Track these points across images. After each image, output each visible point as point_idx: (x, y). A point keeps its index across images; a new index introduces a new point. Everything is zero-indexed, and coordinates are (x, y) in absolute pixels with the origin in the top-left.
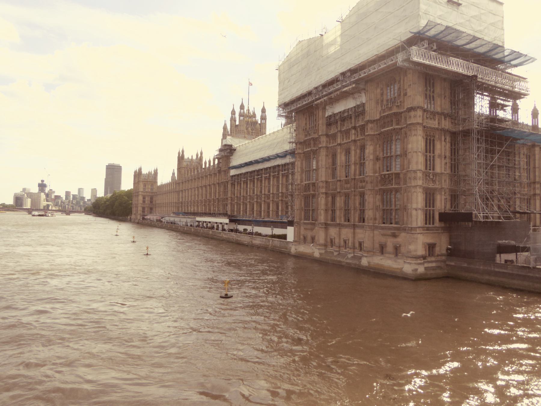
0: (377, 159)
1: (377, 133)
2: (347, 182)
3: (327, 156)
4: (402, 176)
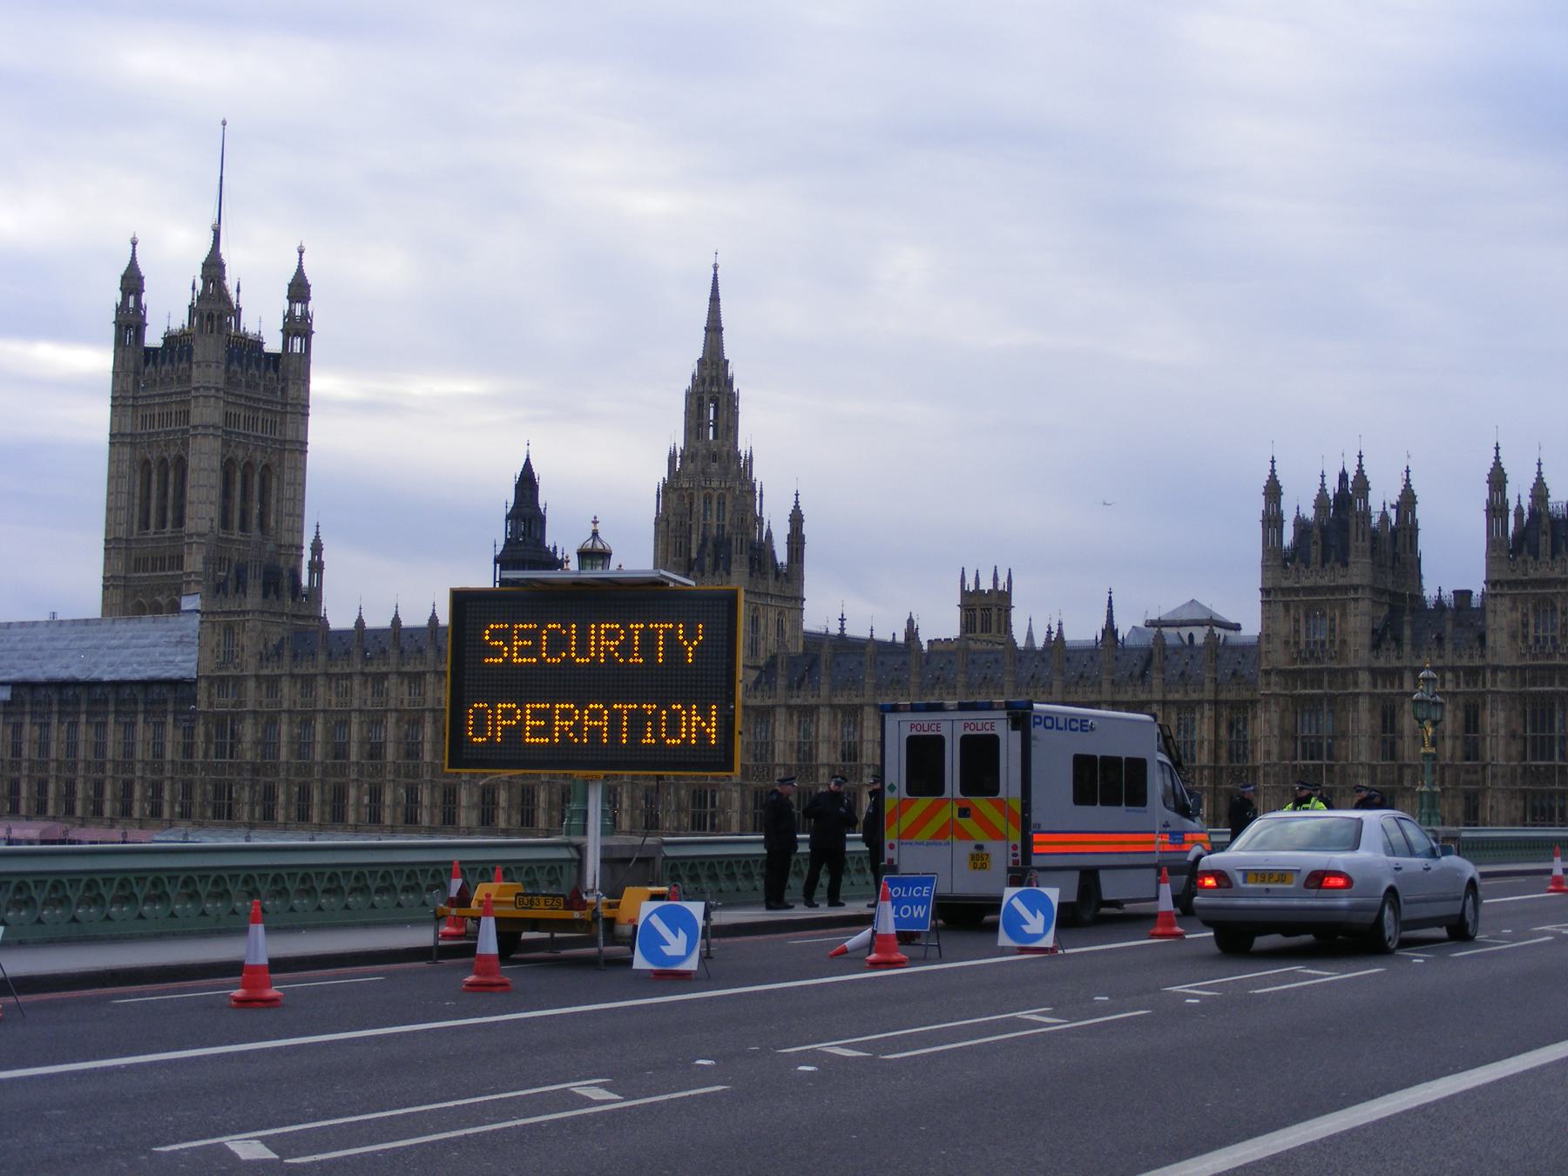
0: (1513, 735)
1: (1517, 690)
3: (1371, 710)
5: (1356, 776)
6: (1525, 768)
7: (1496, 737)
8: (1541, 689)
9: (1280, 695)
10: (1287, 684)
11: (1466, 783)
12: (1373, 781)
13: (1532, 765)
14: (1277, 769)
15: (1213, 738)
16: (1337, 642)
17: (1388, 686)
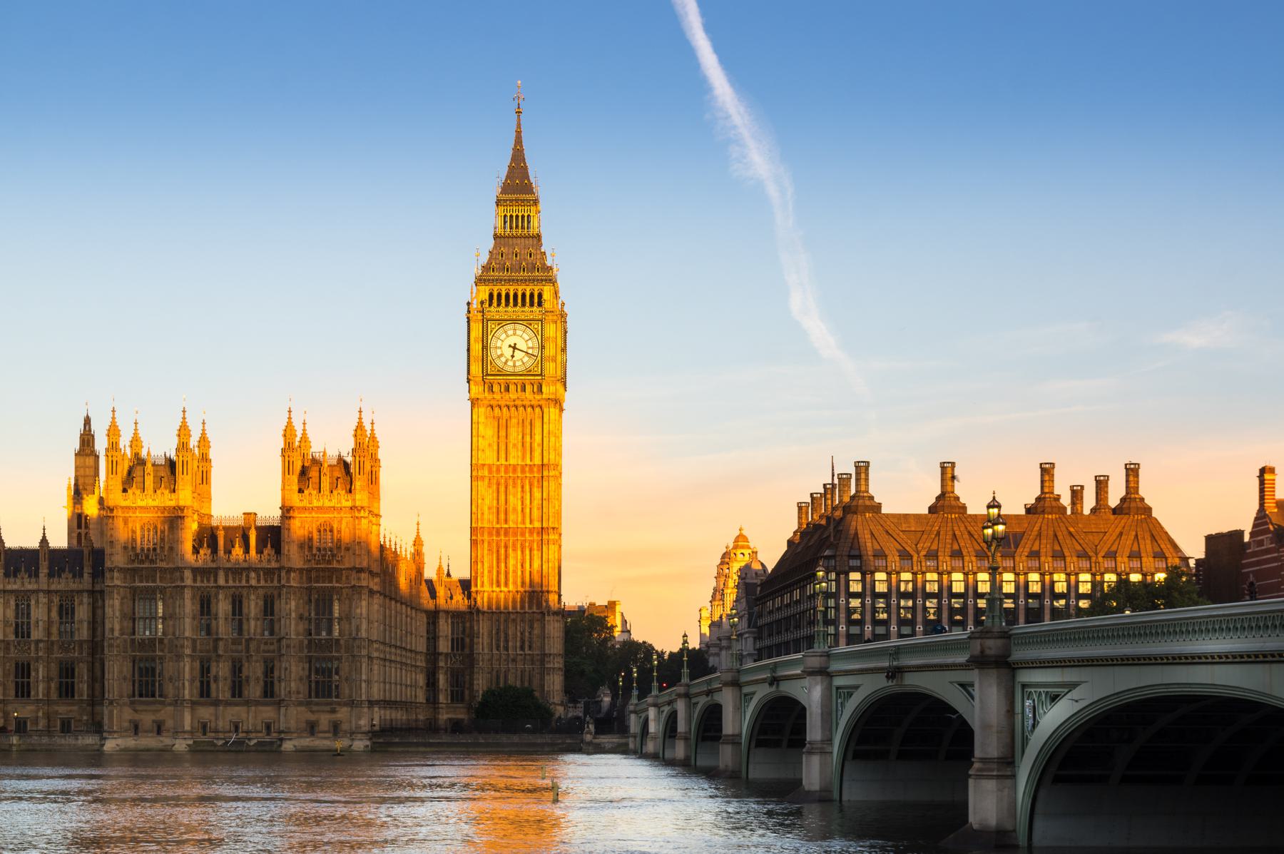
0: (301, 617)
1: (305, 585)
2: (234, 642)
3: (193, 598)
4: (342, 642)
5: (182, 646)
6: (310, 641)
7: (290, 618)
8: (321, 585)
9: (121, 587)
10: (125, 578)
11: (264, 651)
12: (194, 650)
13: (315, 639)
14: (118, 641)
15: (46, 619)
16: (167, 548)
17: (205, 581)
